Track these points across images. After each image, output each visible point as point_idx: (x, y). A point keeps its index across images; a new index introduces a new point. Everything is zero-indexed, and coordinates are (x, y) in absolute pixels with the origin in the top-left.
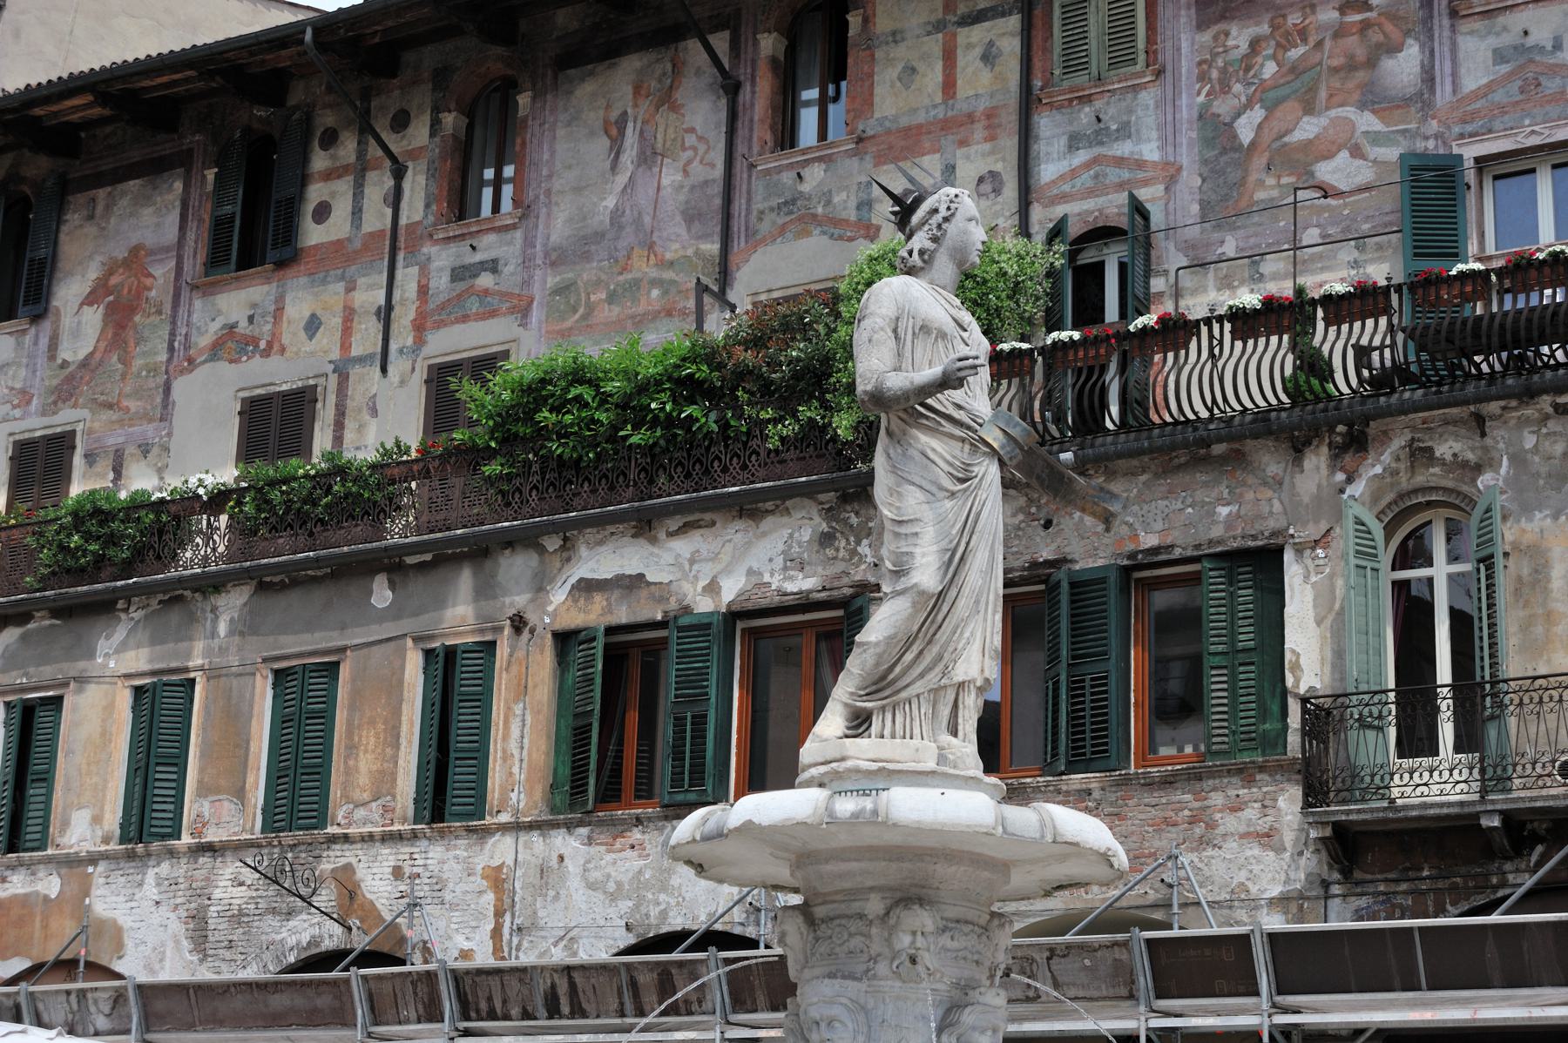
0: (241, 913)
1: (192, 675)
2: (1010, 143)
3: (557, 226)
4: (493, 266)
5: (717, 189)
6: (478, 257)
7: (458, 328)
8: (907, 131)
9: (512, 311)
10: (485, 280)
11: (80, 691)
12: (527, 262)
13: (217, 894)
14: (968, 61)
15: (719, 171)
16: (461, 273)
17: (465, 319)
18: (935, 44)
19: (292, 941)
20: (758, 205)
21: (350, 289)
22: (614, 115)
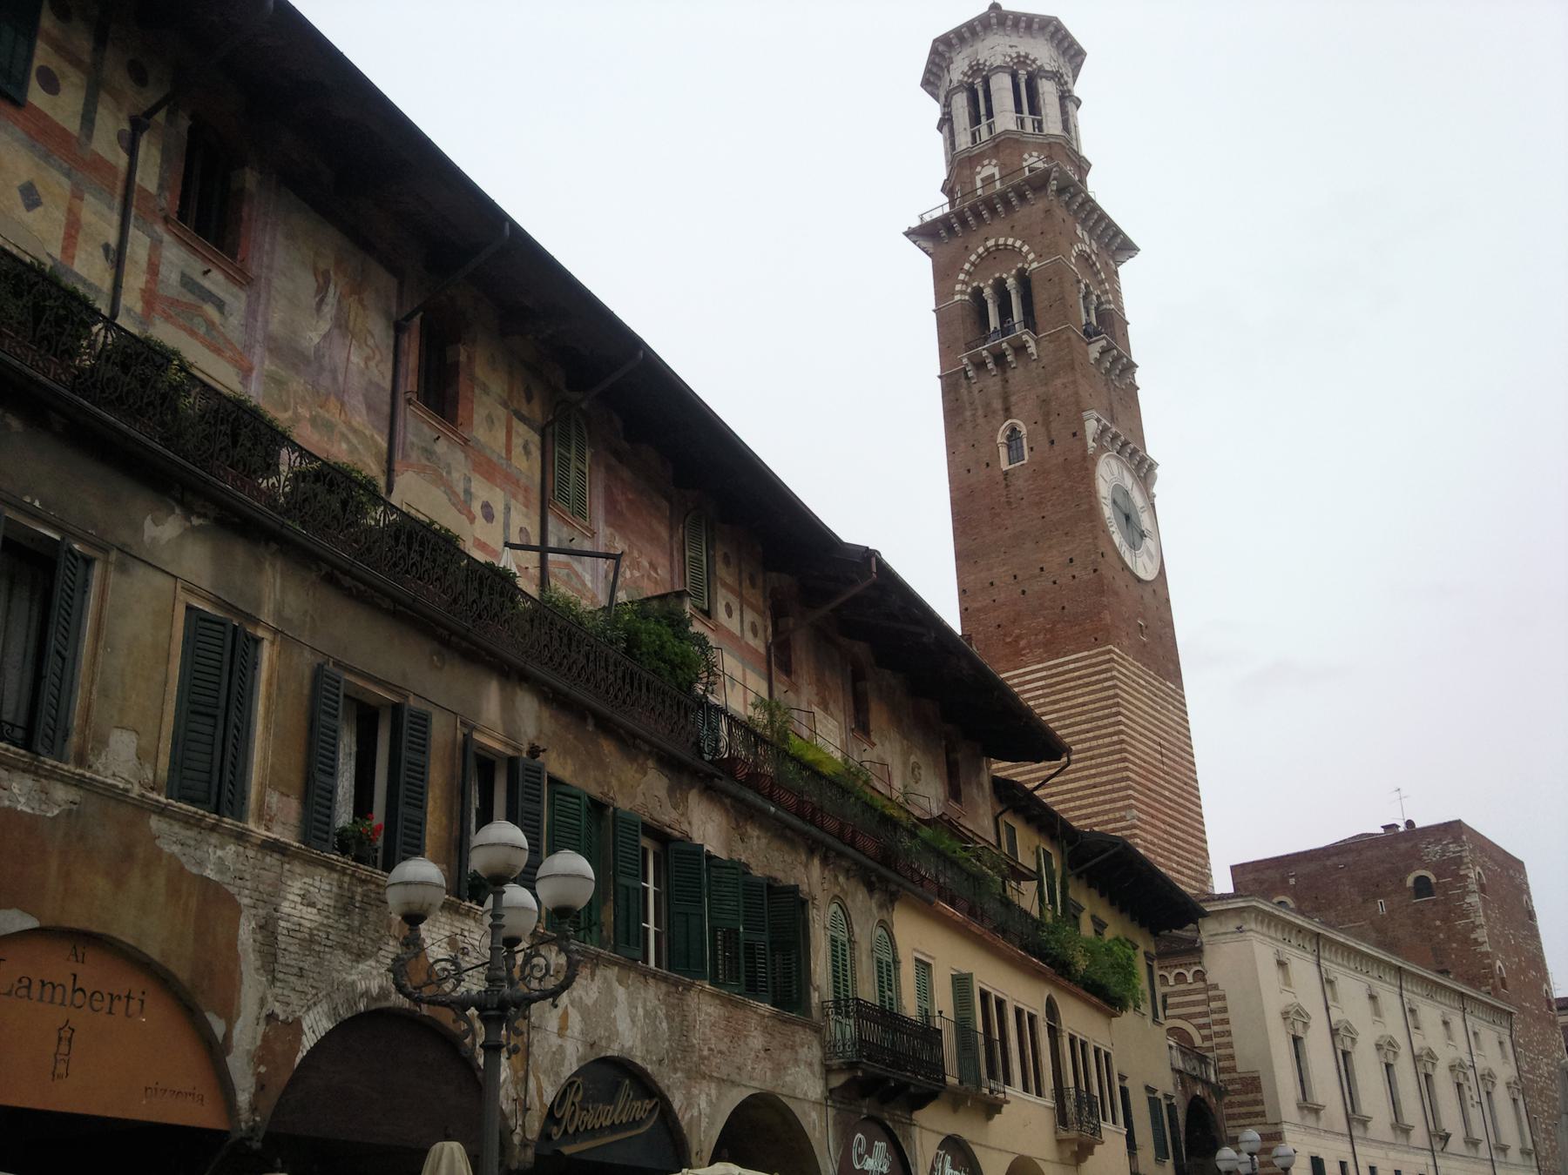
0: (311, 940)
1: (260, 633)
2: (537, 519)
3: (276, 319)
4: (220, 305)
5: (388, 398)
6: (206, 283)
7: (184, 336)
8: (489, 461)
9: (235, 363)
10: (210, 310)
11: (122, 569)
12: (248, 327)
13: (286, 907)
14: (517, 442)
15: (387, 385)
16: (187, 282)
17: (192, 333)
18: (501, 412)
19: (361, 986)
20: (411, 438)
21: (77, 195)
22: (322, 266)
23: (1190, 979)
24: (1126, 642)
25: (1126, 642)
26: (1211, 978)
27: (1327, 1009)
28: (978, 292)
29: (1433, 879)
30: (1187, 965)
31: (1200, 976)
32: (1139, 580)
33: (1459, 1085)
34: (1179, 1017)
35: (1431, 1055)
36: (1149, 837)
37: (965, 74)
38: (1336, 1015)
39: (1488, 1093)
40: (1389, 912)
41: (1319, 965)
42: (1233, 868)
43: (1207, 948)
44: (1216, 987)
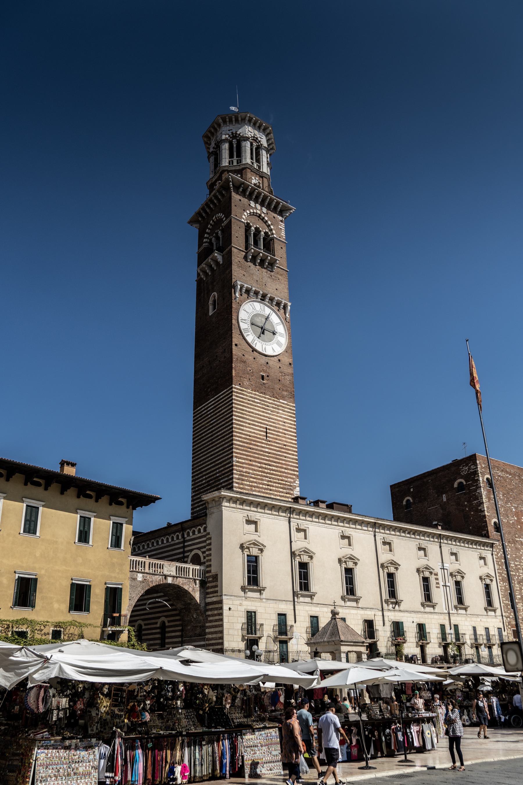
23: (202, 531)
24: (246, 383)
25: (246, 383)
26: (208, 530)
27: (291, 542)
28: (211, 240)
29: (465, 483)
30: (201, 525)
31: (205, 530)
32: (266, 356)
33: (426, 580)
34: (198, 549)
35: (396, 565)
36: (244, 470)
37: (214, 148)
38: (297, 546)
39: (458, 584)
40: (447, 500)
41: (289, 522)
42: (391, 486)
43: (208, 516)
44: (209, 534)
